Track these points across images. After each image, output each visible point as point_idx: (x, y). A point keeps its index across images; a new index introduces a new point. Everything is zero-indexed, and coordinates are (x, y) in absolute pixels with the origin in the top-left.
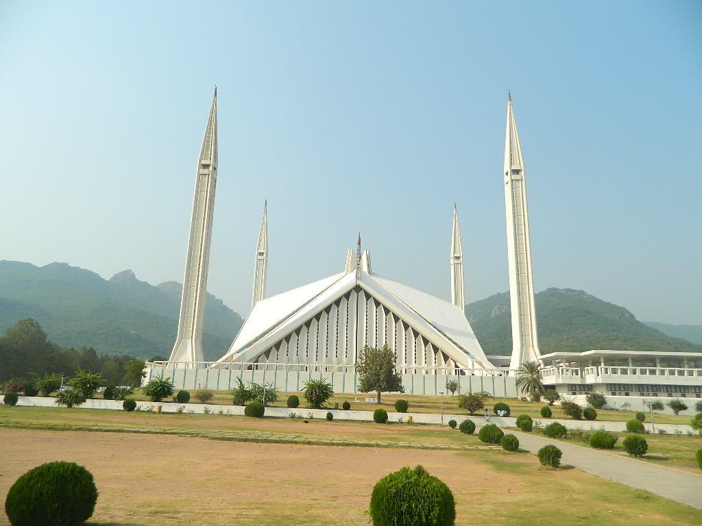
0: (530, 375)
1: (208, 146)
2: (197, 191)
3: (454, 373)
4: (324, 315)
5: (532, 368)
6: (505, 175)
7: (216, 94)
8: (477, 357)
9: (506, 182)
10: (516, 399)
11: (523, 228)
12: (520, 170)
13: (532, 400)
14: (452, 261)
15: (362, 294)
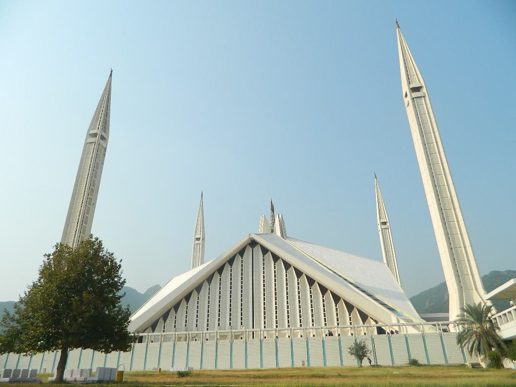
0: (478, 325)
1: (98, 118)
2: (82, 159)
3: (376, 332)
4: (217, 275)
5: (476, 314)
6: (405, 98)
7: (111, 75)
8: (405, 314)
9: (406, 105)
10: (462, 366)
11: (438, 156)
12: (421, 87)
13: (490, 366)
14: (379, 226)
15: (258, 250)
